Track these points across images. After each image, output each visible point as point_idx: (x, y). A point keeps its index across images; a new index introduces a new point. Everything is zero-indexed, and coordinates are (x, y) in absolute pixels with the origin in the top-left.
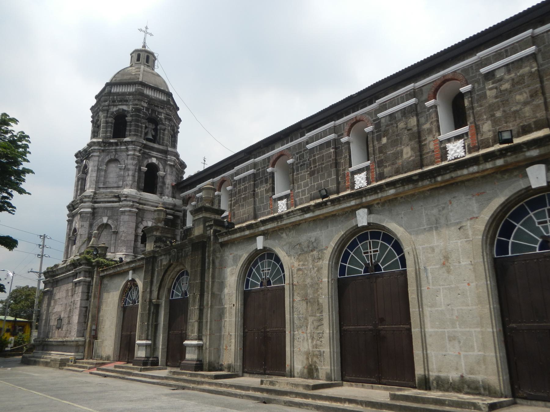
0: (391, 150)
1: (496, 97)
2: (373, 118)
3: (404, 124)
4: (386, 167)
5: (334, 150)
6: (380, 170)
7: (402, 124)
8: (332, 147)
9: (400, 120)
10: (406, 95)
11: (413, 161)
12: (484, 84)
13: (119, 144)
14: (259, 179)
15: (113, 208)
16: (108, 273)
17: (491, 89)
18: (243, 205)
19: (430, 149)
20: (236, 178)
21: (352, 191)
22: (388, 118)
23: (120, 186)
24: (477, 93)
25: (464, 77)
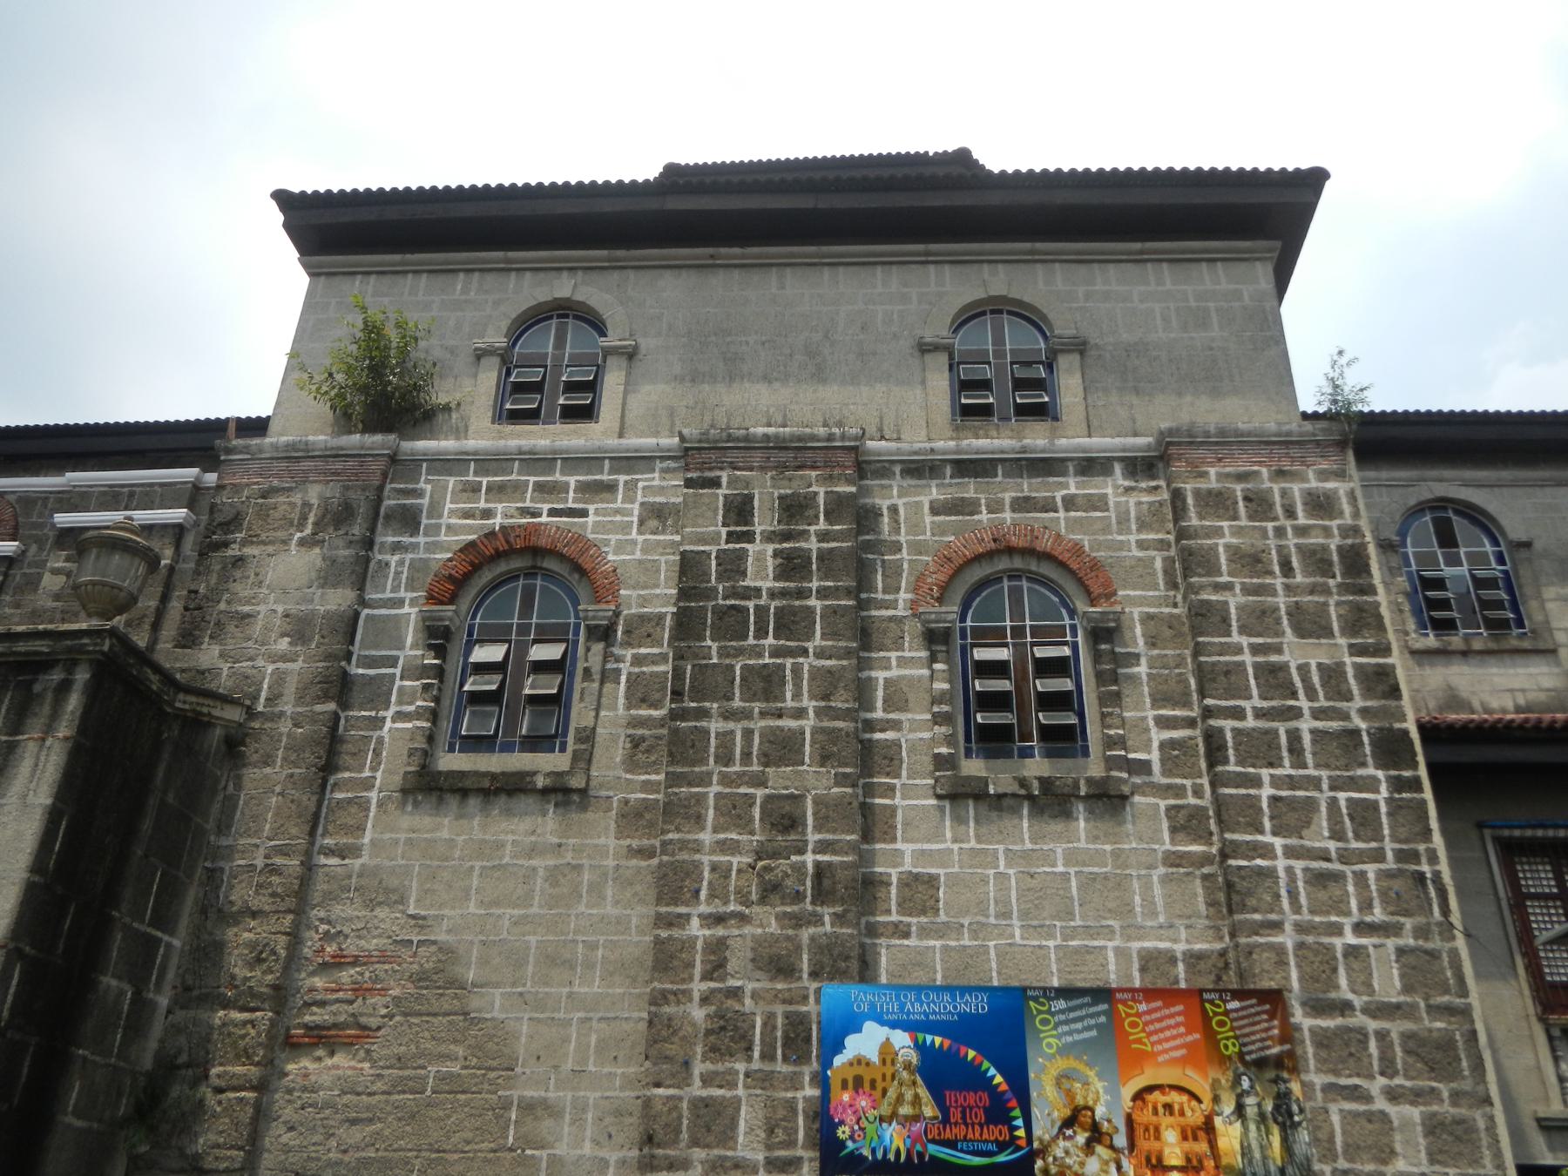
1: (57, 597)
12: (50, 551)
17: (56, 572)
24: (28, 571)
25: (15, 516)
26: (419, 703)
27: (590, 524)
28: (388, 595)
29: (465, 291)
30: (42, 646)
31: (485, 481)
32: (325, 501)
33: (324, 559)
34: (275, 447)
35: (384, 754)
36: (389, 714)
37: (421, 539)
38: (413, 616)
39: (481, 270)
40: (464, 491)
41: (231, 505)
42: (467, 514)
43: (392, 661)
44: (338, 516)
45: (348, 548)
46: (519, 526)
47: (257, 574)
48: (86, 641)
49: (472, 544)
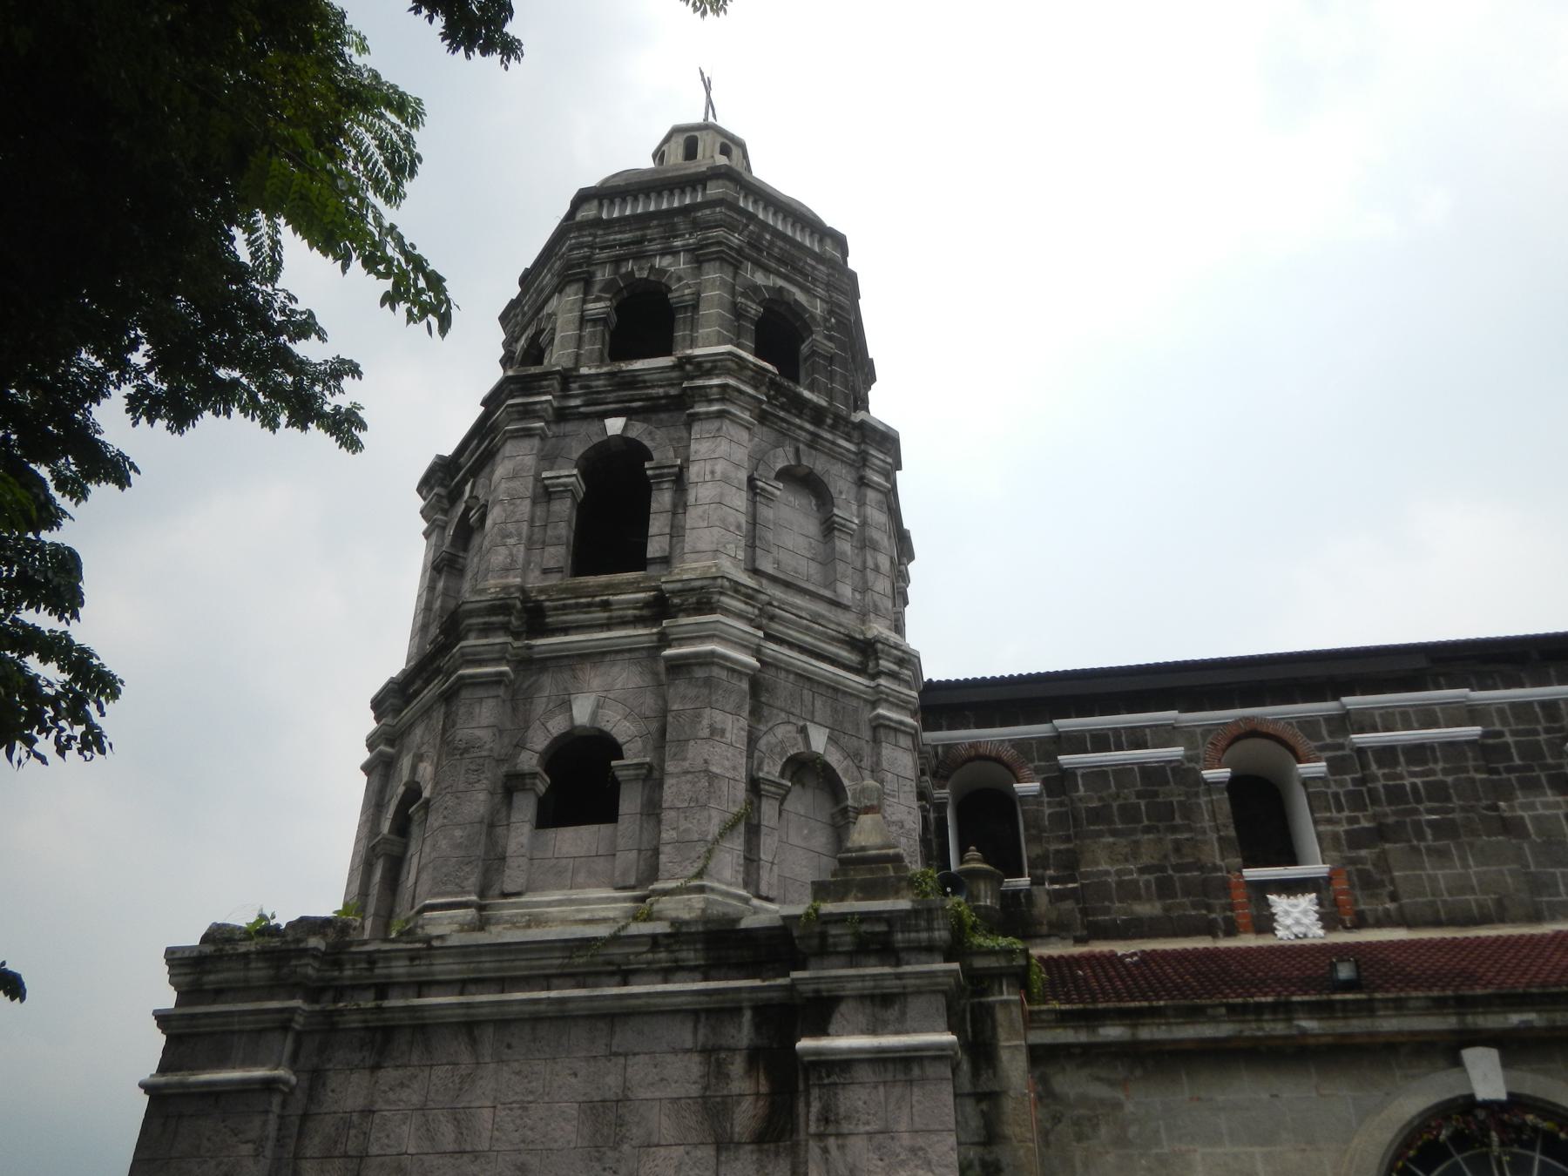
13: (829, 421)
14: (1509, 770)
15: (836, 690)
16: (1145, 1034)
18: (1441, 855)
20: (1358, 738)
23: (845, 602)
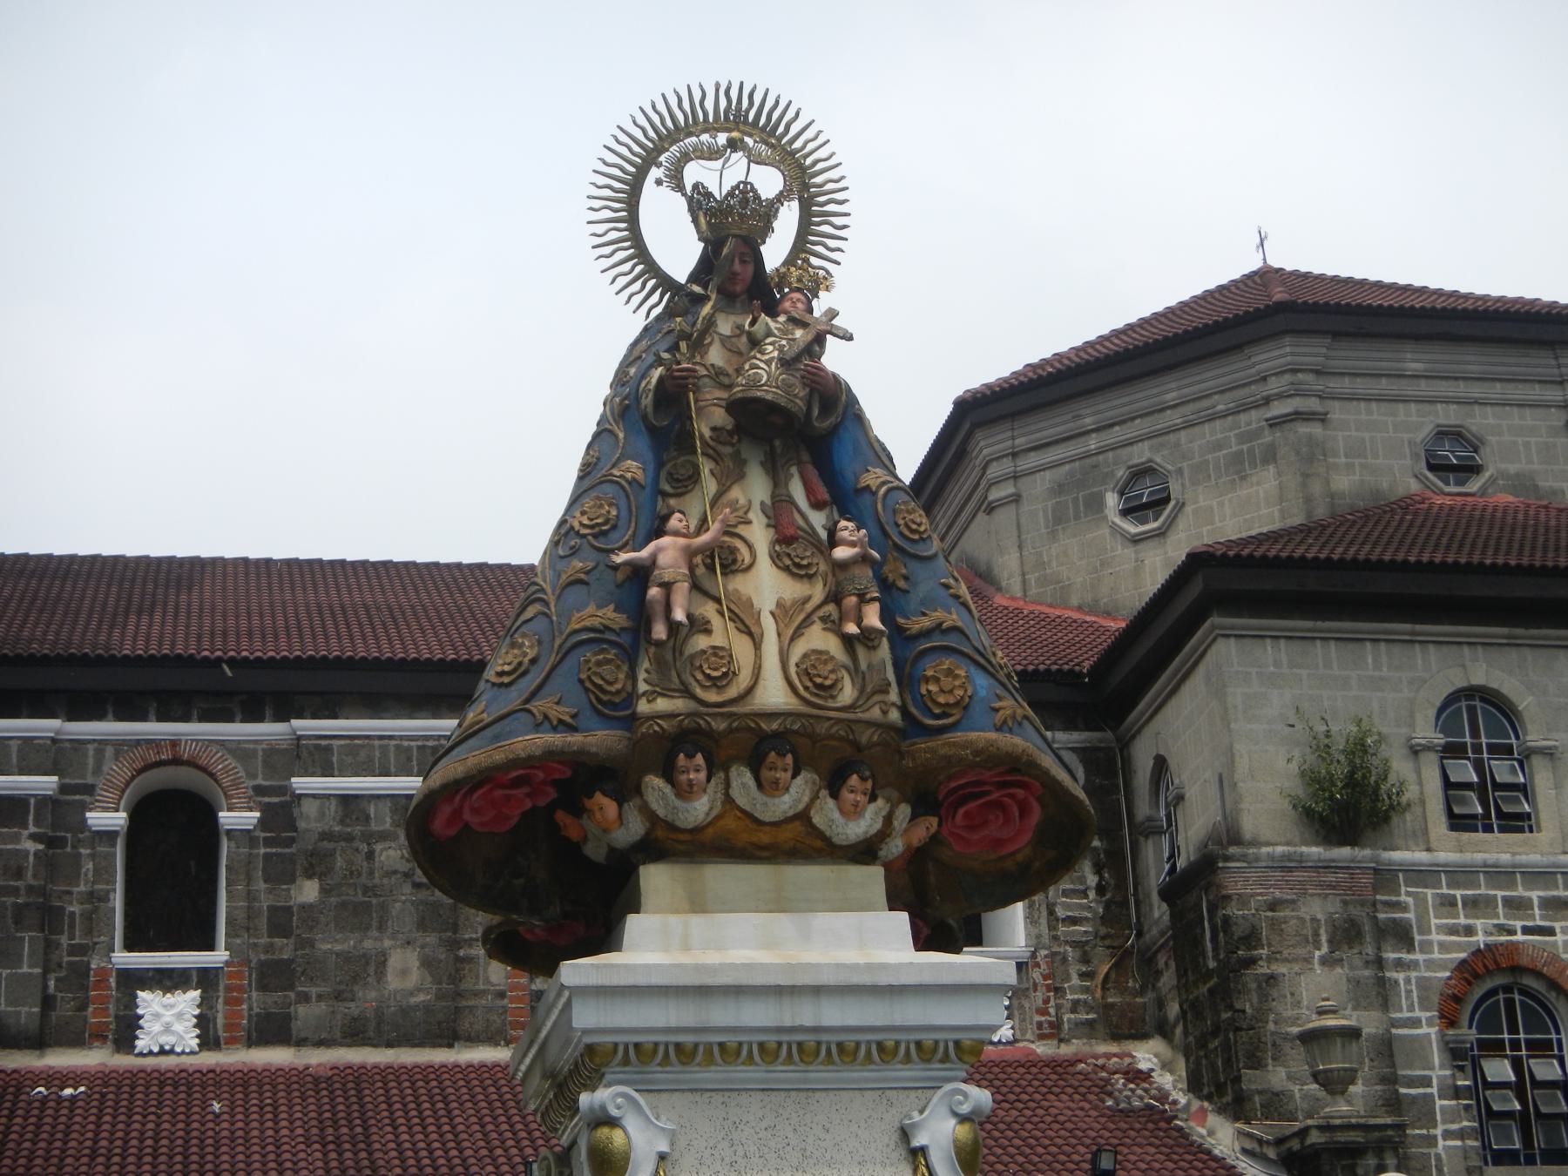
0: (336, 941)
2: (254, 776)
3: (402, 857)
4: (305, 998)
5: (41, 847)
6: (269, 1001)
7: (391, 852)
8: (32, 829)
9: (384, 836)
10: (419, 747)
11: (427, 1009)
19: (486, 980)
21: (123, 1061)
22: (333, 808)
26: (1466, 1123)
27: (1560, 943)
28: (1405, 1014)
29: (1377, 666)
30: (1357, 1137)
31: (1458, 893)
32: (1331, 921)
33: (1348, 980)
34: (1271, 857)
35: (1445, 1169)
36: (1438, 1131)
37: (1418, 956)
38: (1433, 1036)
39: (1387, 641)
40: (1442, 904)
41: (1244, 917)
42: (1453, 930)
43: (1426, 1082)
44: (1346, 934)
45: (1367, 968)
46: (1502, 944)
47: (1292, 994)
48: (1390, 1133)
49: (1463, 962)
